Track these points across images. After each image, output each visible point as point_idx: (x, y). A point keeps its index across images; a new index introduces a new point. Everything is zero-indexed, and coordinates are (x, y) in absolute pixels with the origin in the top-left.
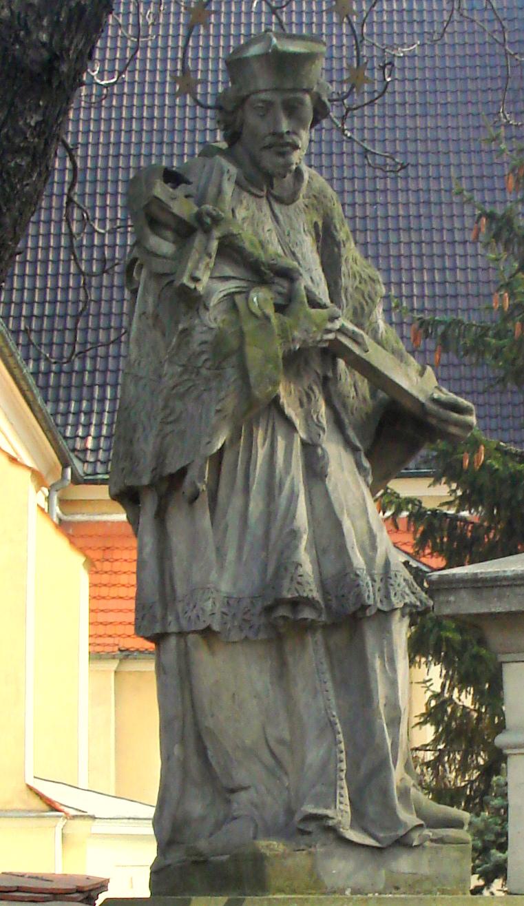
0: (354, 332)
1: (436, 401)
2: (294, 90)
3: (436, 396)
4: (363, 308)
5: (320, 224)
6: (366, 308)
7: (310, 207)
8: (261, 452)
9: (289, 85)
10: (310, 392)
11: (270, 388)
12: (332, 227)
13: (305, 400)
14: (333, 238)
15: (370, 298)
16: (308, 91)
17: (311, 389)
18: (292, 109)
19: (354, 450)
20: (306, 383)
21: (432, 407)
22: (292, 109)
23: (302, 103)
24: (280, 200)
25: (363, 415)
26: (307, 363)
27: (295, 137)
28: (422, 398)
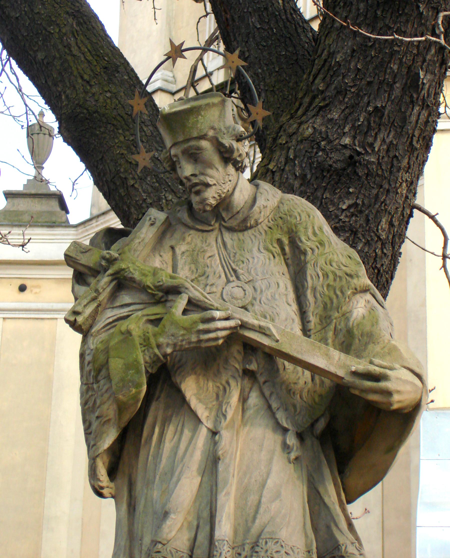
0: (260, 327)
1: (355, 374)
2: (188, 140)
3: (353, 369)
4: (332, 303)
5: (286, 241)
6: (335, 301)
7: (275, 228)
8: (168, 445)
9: (181, 139)
10: (227, 386)
11: (134, 390)
12: (297, 239)
13: (221, 393)
14: (298, 248)
15: (342, 292)
16: (203, 137)
17: (228, 383)
18: (194, 156)
19: (285, 430)
20: (224, 379)
21: (348, 379)
22: (194, 156)
23: (199, 148)
24: (231, 230)
25: (317, 399)
26: (226, 361)
27: (202, 178)
28: (341, 373)
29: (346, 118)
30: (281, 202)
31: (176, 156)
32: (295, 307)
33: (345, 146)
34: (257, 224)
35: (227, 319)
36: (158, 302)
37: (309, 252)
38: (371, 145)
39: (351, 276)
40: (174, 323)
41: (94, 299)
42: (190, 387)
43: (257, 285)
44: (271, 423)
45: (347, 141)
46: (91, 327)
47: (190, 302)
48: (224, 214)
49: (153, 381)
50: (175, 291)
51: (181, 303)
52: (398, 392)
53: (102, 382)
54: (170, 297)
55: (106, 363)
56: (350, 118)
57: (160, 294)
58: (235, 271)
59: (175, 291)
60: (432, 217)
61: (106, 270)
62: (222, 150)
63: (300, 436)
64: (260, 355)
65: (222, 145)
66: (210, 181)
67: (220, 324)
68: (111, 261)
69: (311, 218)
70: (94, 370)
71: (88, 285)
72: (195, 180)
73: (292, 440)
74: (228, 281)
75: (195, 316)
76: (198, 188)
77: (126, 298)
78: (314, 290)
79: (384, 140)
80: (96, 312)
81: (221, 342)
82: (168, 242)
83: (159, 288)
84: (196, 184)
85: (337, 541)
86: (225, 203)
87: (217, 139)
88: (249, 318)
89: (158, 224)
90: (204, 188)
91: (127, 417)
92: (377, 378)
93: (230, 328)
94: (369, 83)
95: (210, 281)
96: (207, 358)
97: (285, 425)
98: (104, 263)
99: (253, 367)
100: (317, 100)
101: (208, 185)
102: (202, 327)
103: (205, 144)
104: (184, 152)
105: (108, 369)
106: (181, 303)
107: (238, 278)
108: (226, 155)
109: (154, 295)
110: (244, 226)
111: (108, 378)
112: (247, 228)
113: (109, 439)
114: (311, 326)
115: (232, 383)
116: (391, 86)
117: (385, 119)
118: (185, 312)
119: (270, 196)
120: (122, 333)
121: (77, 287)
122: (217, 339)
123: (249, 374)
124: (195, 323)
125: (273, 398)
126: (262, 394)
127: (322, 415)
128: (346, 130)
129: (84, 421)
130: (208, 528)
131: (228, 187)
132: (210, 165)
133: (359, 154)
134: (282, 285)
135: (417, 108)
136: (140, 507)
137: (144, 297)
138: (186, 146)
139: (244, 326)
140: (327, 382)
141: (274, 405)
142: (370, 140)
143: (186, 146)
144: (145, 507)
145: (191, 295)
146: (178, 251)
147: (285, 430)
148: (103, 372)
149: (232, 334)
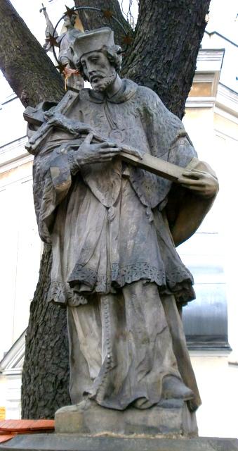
1: (184, 176)
5: (141, 109)
17: (114, 182)
20: (112, 179)
24: (112, 103)
26: (113, 171)
29: (152, 66)
30: (138, 89)
31: (84, 61)
32: (147, 144)
33: (153, 80)
35: (115, 147)
37: (155, 115)
38: (165, 79)
39: (177, 128)
42: (93, 185)
43: (128, 131)
44: (137, 203)
45: (153, 77)
46: (39, 151)
47: (94, 138)
48: (110, 96)
49: (74, 178)
50: (86, 132)
51: (88, 138)
52: (209, 185)
53: (46, 180)
54: (83, 136)
56: (155, 66)
57: (77, 134)
58: (115, 124)
59: (86, 132)
61: (46, 121)
62: (110, 58)
63: (153, 210)
65: (109, 55)
67: (112, 149)
68: (50, 117)
69: (154, 101)
70: (40, 177)
71: (36, 130)
72: (95, 74)
73: (149, 212)
74: (112, 129)
76: (96, 79)
77: (57, 136)
79: (171, 78)
81: (111, 159)
82: (78, 109)
83: (76, 130)
84: (95, 77)
85: (175, 265)
86: (110, 87)
87: (107, 52)
89: (74, 99)
90: (99, 79)
91: (61, 199)
92: (196, 178)
93: (116, 152)
94: (165, 48)
97: (145, 203)
98: (46, 117)
100: (137, 57)
101: (102, 77)
102: (102, 150)
103: (101, 55)
104: (90, 59)
105: (50, 172)
107: (117, 128)
108: (112, 61)
109: (73, 134)
110: (122, 101)
113: (49, 212)
115: (117, 182)
116: (175, 50)
117: (172, 67)
118: (91, 143)
119: (133, 87)
120: (58, 154)
121: (30, 131)
122: (109, 157)
123: (124, 177)
125: (138, 190)
127: (164, 200)
128: (153, 72)
129: (35, 202)
130: (106, 258)
131: (112, 79)
132: (103, 66)
133: (159, 83)
134: (140, 132)
135: (187, 63)
136: (66, 248)
139: (123, 151)
140: (167, 182)
141: (139, 194)
142: (165, 77)
144: (69, 248)
145: (95, 134)
147: (146, 207)
148: (48, 175)
149: (116, 156)
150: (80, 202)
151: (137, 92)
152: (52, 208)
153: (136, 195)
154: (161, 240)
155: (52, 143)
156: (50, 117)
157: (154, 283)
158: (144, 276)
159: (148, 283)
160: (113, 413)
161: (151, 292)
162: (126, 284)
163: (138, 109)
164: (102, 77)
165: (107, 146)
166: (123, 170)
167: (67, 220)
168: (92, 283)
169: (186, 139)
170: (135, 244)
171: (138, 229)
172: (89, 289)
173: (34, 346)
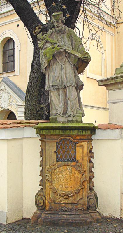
16: (60, 19)
21: (82, 58)
30: (69, 29)
34: (66, 33)
36: (53, 45)
40: (56, 48)
41: (43, 44)
44: (69, 64)
51: (57, 45)
55: (46, 54)
59: (56, 43)
60: (78, 29)
61: (44, 39)
63: (73, 65)
64: (67, 53)
66: (60, 26)
73: (72, 66)
75: (60, 47)
77: (47, 44)
78: (74, 43)
80: (43, 46)
83: (53, 43)
88: (67, 48)
89: (51, 32)
95: (59, 42)
96: (60, 54)
97: (71, 64)
99: (67, 55)
101: (59, 27)
102: (60, 49)
103: (60, 20)
104: (56, 21)
106: (57, 45)
111: (46, 56)
112: (64, 33)
114: (74, 49)
123: (66, 56)
124: (60, 49)
126: (68, 59)
137: (51, 44)
138: (56, 20)
139: (66, 49)
141: (70, 61)
143: (56, 20)
146: (54, 37)
147: (72, 65)
148: (45, 56)
150: (54, 63)
151: (68, 30)
152: (47, 65)
153: (69, 61)
154: (75, 74)
155: (46, 46)
156: (45, 38)
157: (75, 86)
158: (72, 84)
159: (74, 86)
160: (64, 118)
161: (74, 88)
162: (68, 86)
163: (69, 36)
164: (59, 27)
165: (62, 48)
166: (66, 54)
167: (50, 67)
168: (58, 85)
169: (82, 45)
170: (69, 76)
171: (70, 71)
172: (58, 87)
173: (29, 100)
